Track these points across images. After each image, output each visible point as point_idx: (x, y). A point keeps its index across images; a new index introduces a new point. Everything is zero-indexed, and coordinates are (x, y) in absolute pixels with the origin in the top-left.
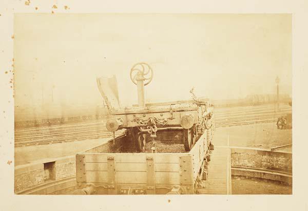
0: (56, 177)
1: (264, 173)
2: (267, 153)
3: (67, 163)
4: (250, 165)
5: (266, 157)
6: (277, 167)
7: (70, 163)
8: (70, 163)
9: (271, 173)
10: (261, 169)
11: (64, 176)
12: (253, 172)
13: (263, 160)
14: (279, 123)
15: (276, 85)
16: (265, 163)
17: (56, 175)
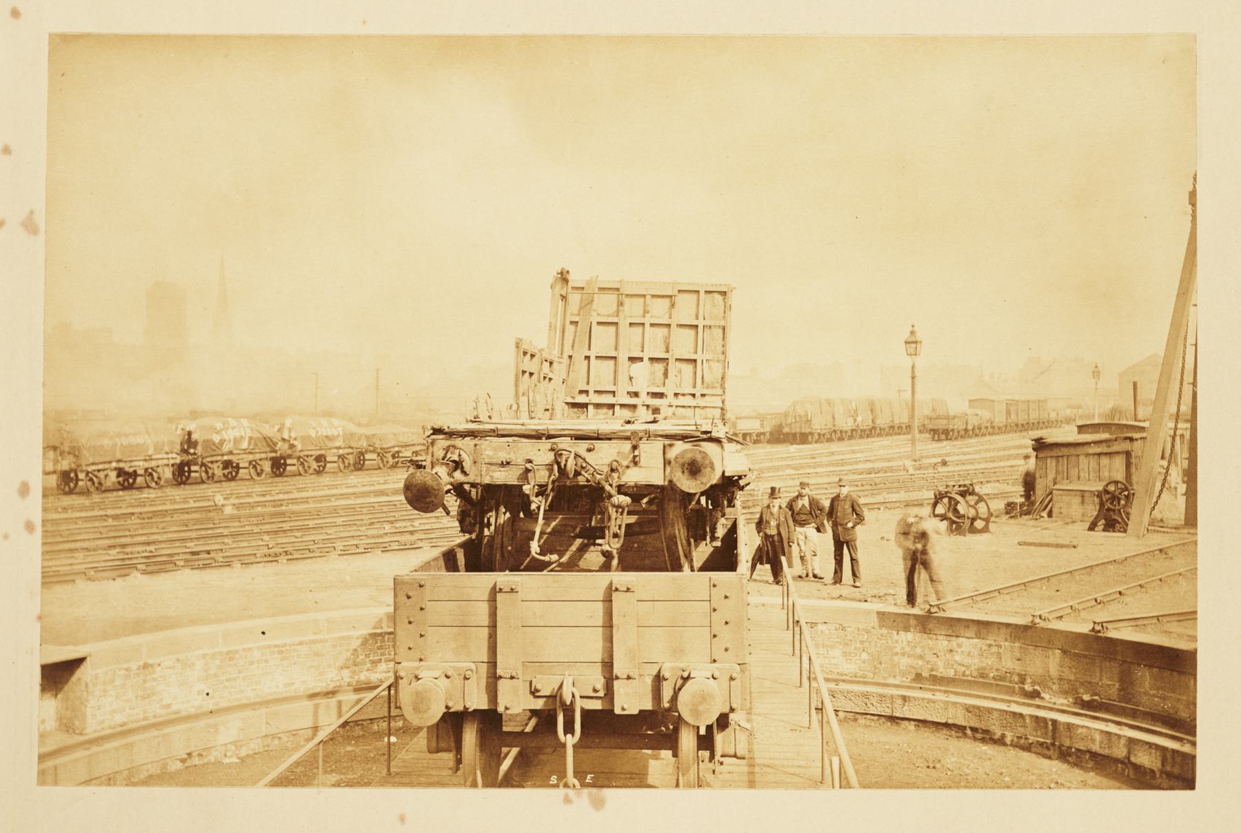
0: (89, 720)
1: (904, 698)
2: (912, 622)
3: (134, 666)
4: (849, 668)
5: (910, 636)
6: (951, 673)
7: (146, 666)
8: (146, 666)
9: (928, 695)
10: (891, 681)
11: (119, 719)
12: (866, 696)
13: (898, 650)
14: (940, 509)
15: (908, 362)
16: (905, 662)
17: (89, 711)
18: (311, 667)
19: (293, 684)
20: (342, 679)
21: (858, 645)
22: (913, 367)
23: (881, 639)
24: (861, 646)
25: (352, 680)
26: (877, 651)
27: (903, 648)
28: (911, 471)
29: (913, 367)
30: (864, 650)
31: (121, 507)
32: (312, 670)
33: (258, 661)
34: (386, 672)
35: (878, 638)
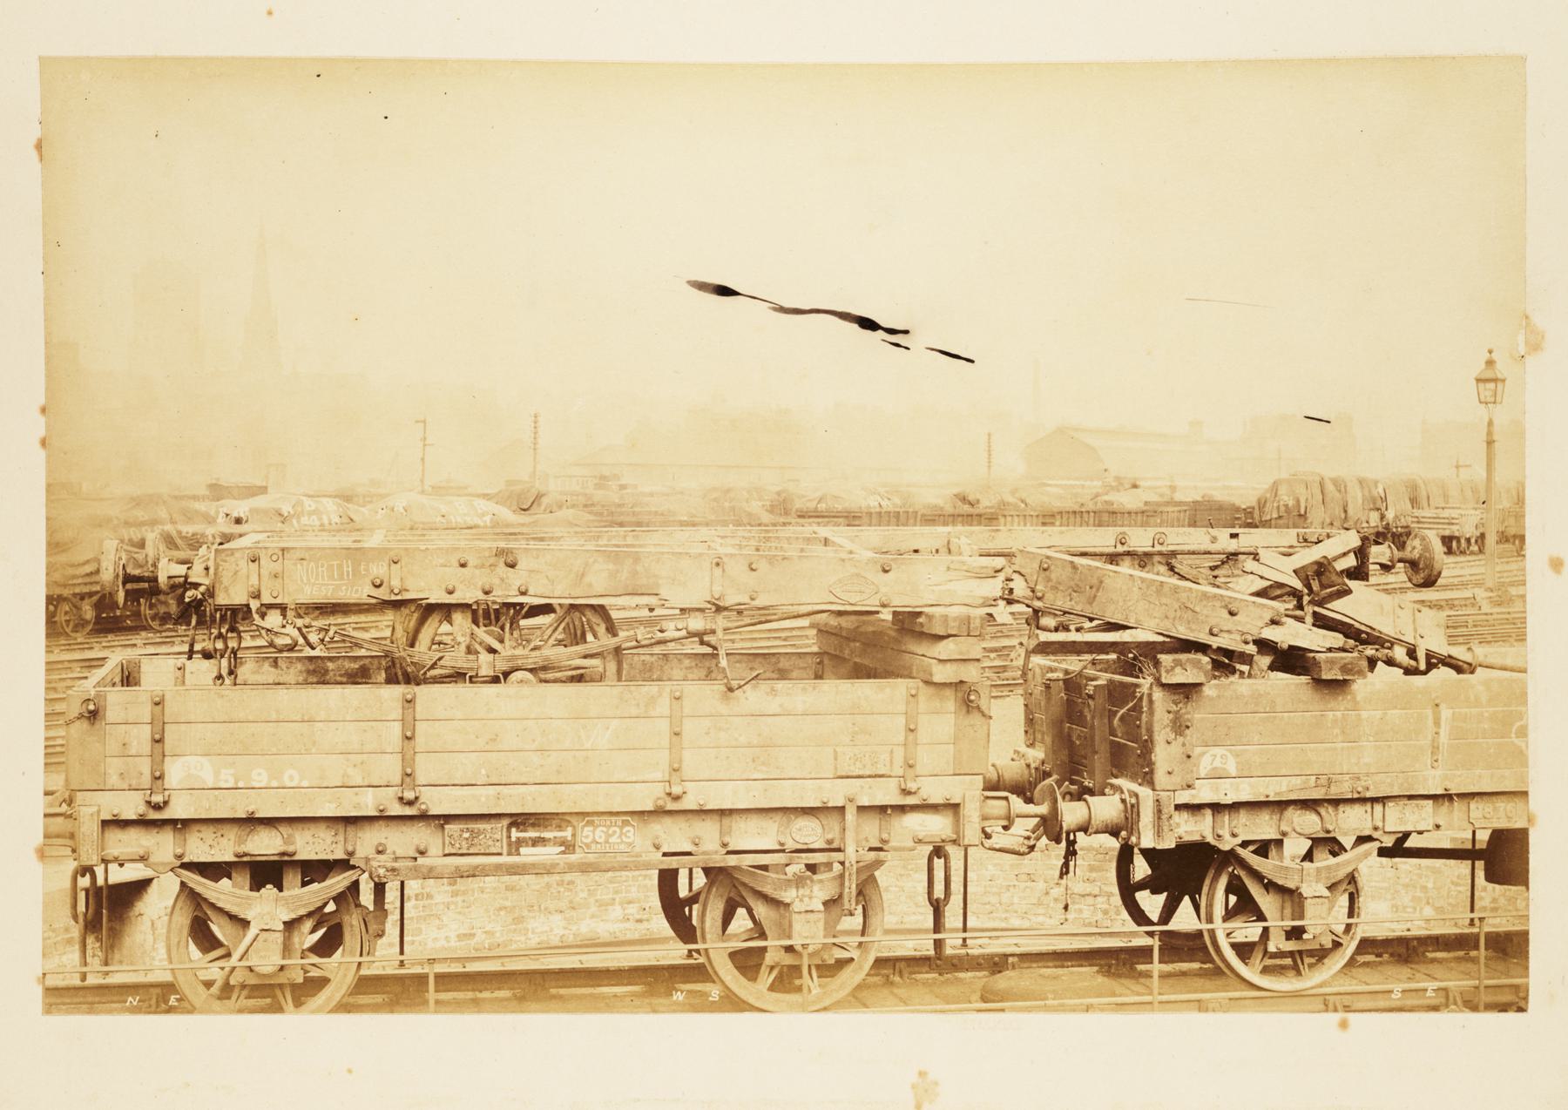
18: (501, 909)
19: (473, 935)
20: (551, 930)
21: (1419, 894)
22: (1490, 423)
23: (1457, 885)
24: (1422, 895)
25: (567, 932)
26: (1450, 904)
27: (1494, 900)
28: (1486, 608)
29: (1490, 423)
30: (1428, 903)
31: (135, 645)
32: (502, 913)
33: (417, 895)
34: (621, 921)
35: (1453, 883)
